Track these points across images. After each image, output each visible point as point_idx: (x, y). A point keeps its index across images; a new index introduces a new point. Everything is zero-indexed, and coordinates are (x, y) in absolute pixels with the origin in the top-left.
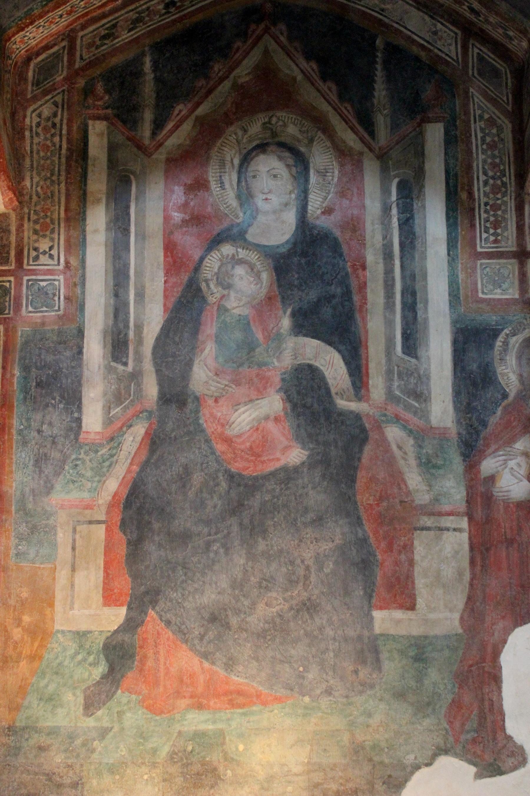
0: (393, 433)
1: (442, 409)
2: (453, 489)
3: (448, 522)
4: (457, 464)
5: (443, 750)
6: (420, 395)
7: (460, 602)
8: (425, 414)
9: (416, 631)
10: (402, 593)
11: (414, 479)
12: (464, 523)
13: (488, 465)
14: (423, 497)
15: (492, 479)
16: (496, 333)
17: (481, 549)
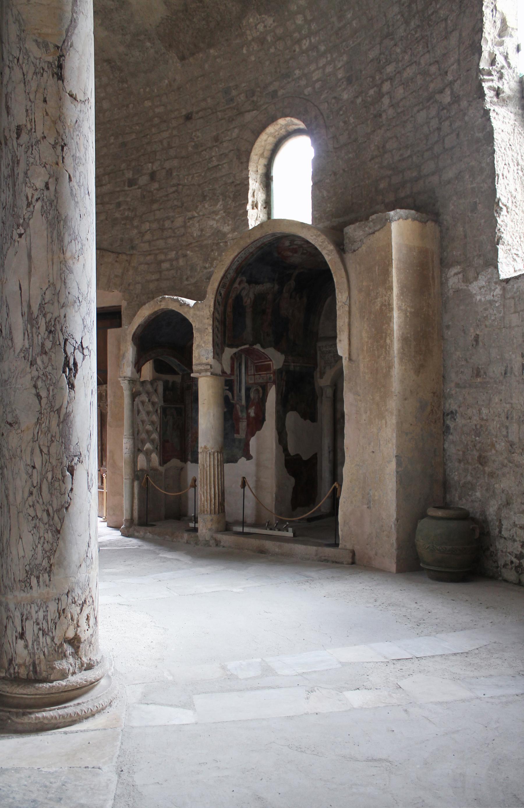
0: (238, 406)
1: (244, 402)
2: (245, 415)
3: (244, 420)
4: (245, 410)
5: (243, 456)
6: (241, 400)
7: (245, 433)
8: (241, 402)
9: (239, 438)
10: (238, 432)
11: (240, 414)
12: (246, 420)
13: (249, 411)
14: (241, 417)
15: (250, 413)
16: (251, 389)
17: (248, 425)
